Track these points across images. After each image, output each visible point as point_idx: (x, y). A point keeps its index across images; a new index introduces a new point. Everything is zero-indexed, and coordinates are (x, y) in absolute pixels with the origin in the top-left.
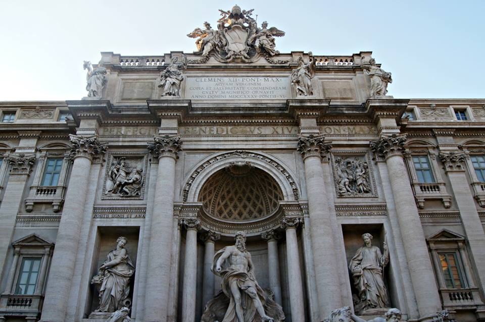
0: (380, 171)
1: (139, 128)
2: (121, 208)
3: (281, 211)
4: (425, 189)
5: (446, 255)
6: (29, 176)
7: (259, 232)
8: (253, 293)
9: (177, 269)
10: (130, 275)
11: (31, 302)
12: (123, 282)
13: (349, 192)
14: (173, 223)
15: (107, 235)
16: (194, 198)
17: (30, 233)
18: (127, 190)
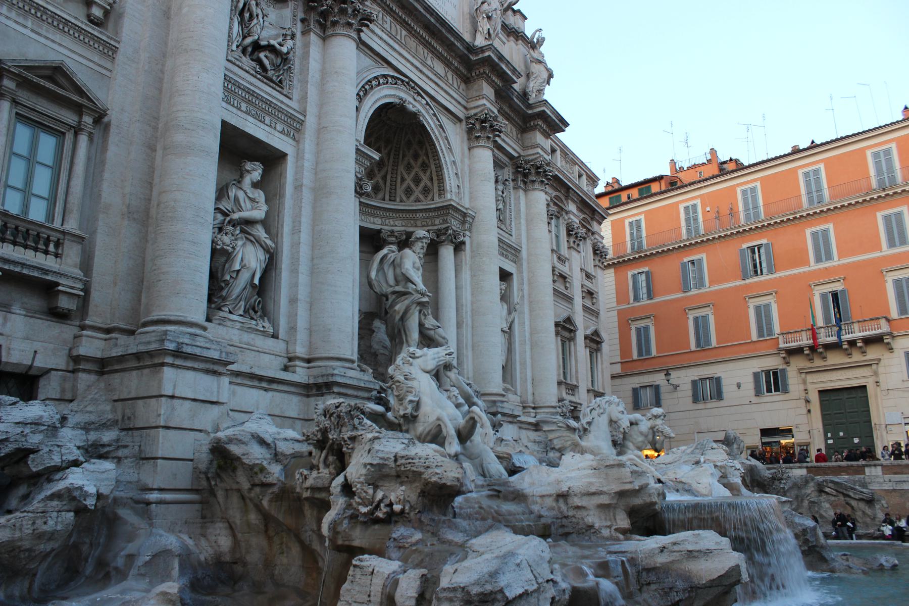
2: (266, 102)
7: (374, 223)
11: (58, 244)
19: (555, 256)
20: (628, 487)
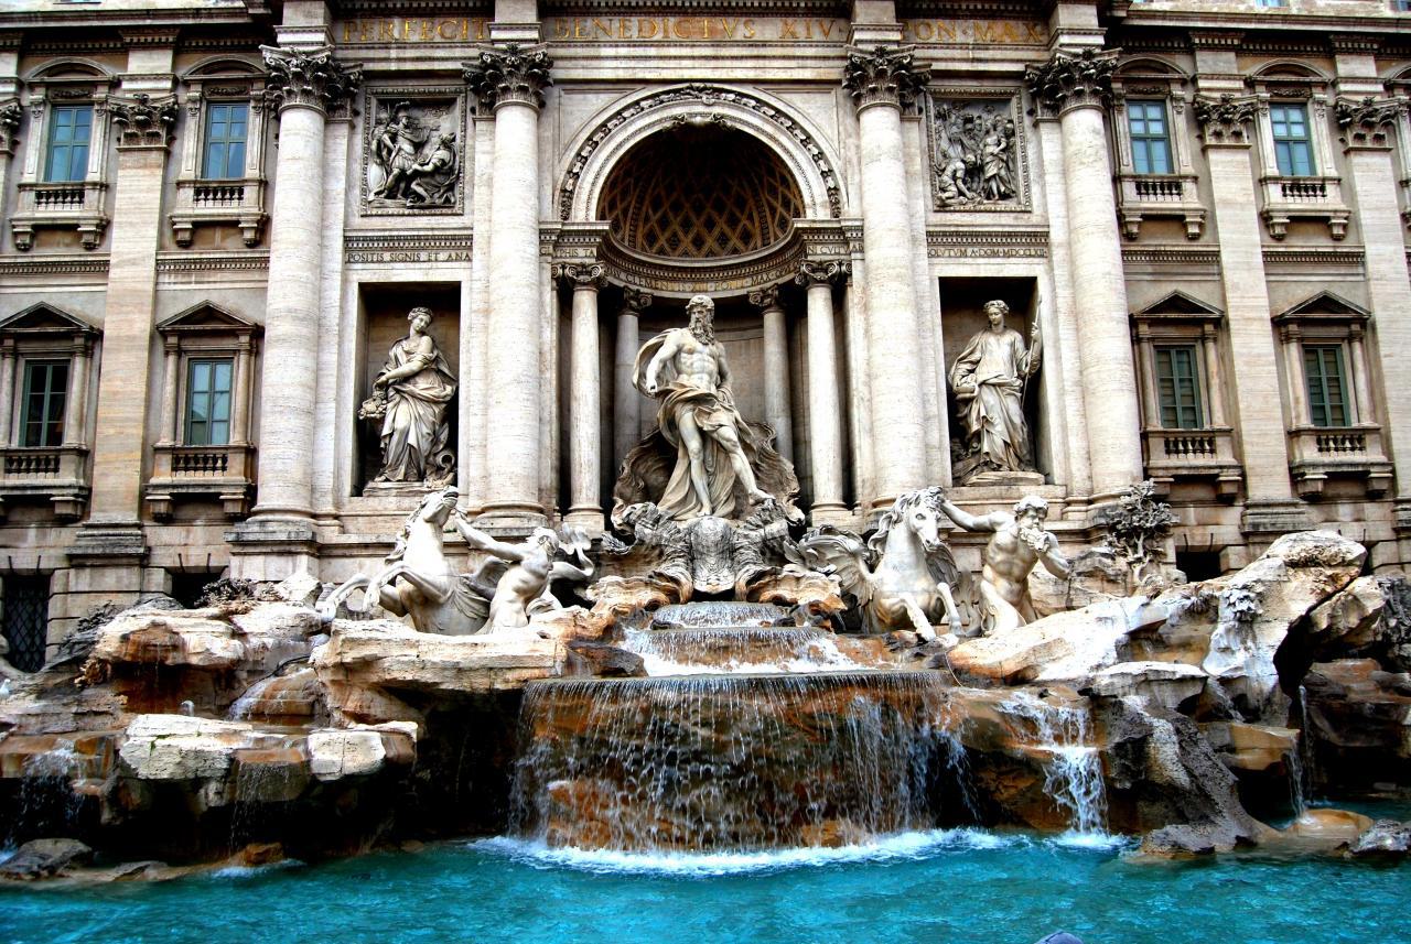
0: (1044, 144)
1: (437, 20)
2: (413, 238)
3: (799, 241)
4: (1147, 187)
5: (1173, 352)
6: (168, 153)
8: (728, 440)
9: (554, 382)
10: (448, 398)
11: (225, 460)
12: (430, 413)
13: (964, 195)
14: (540, 274)
15: (383, 306)
16: (587, 209)
17: (197, 300)
18: (420, 190)
19: (1274, 191)
20: (338, 659)
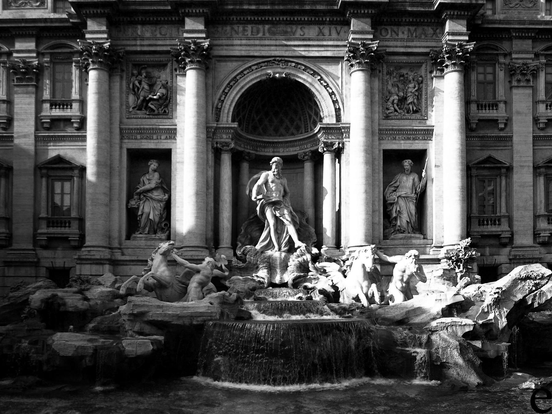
9: (213, 194)
11: (70, 223)
12: (159, 206)
16: (228, 117)
